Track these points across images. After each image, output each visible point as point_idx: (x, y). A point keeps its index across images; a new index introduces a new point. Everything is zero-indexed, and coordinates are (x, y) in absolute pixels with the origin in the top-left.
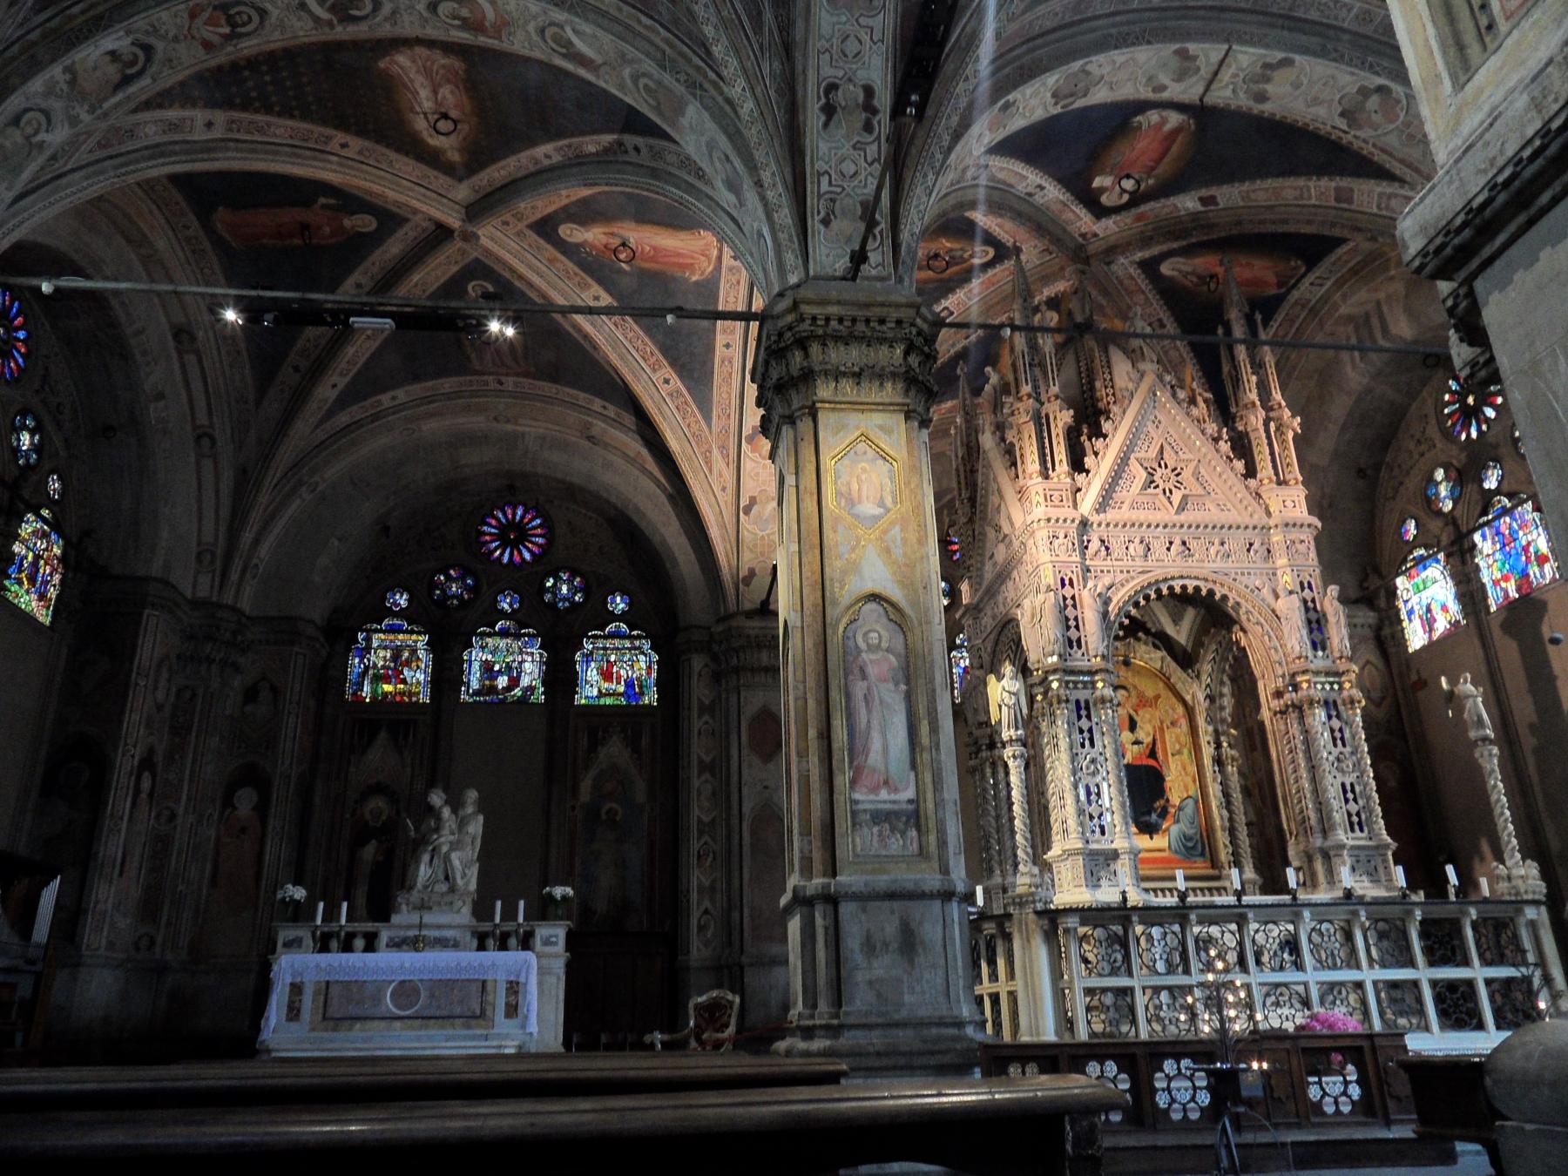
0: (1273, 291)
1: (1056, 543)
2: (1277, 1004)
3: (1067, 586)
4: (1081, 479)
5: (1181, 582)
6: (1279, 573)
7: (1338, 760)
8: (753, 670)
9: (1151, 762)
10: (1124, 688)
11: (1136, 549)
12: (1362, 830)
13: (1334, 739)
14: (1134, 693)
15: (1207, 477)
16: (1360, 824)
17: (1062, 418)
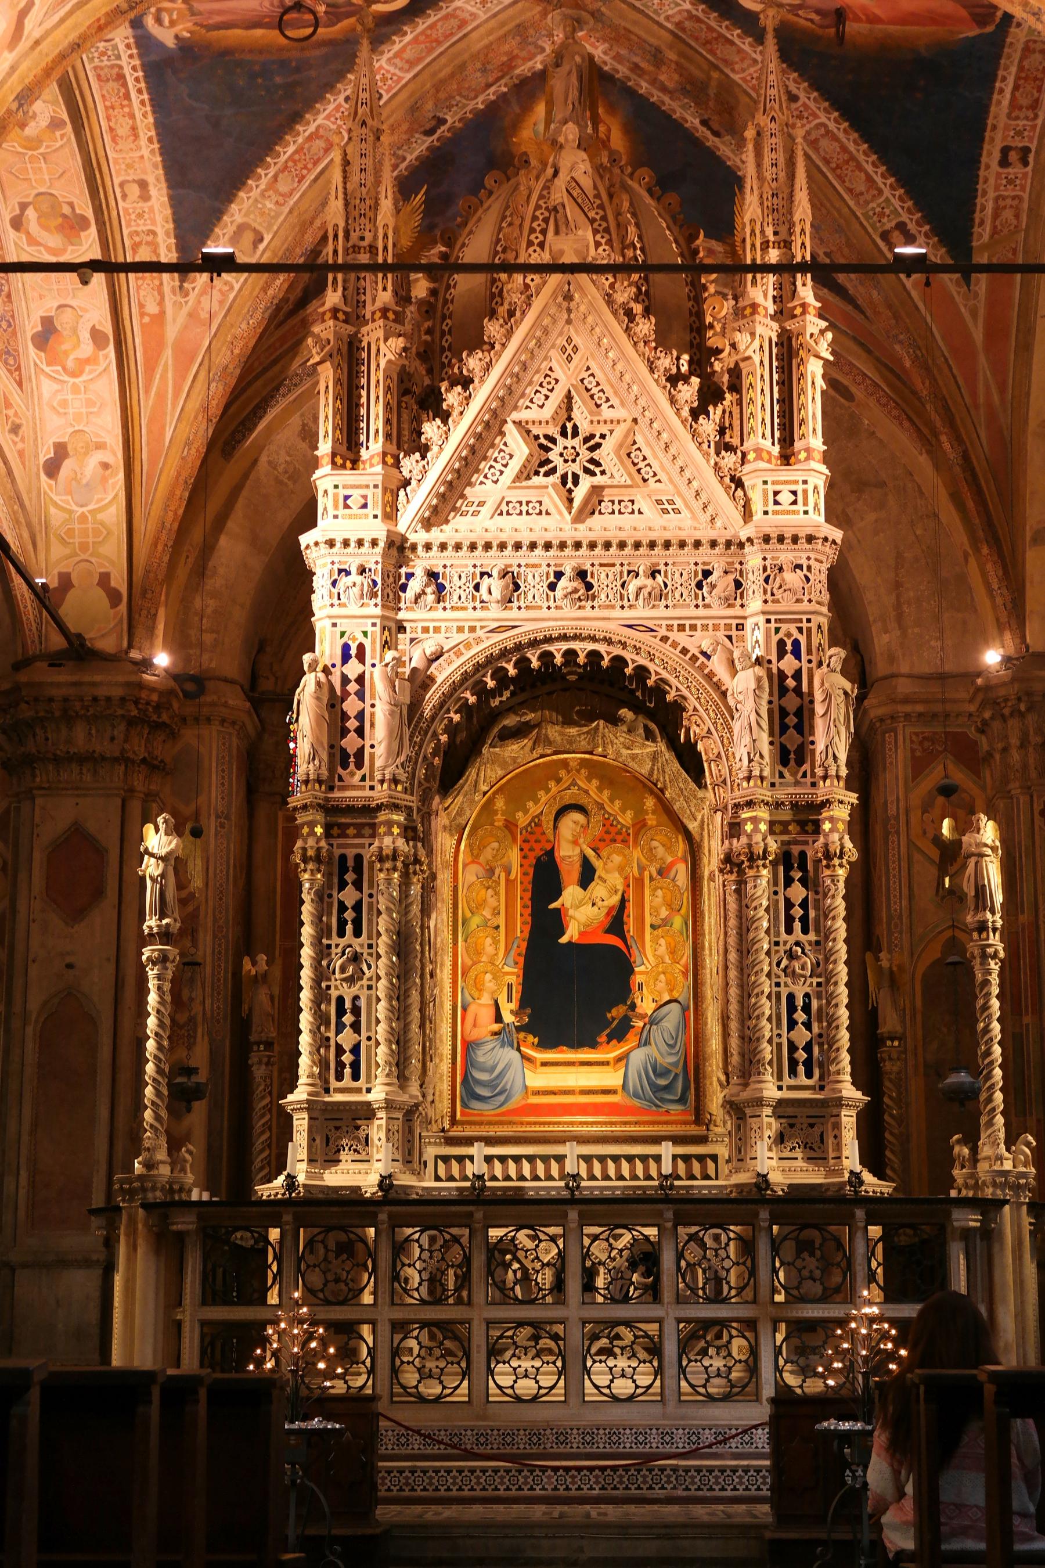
0: (974, 32)
1: (344, 581)
2: (608, 1352)
3: (353, 662)
4: (410, 464)
5: (564, 646)
6: (749, 624)
7: (791, 956)
8: (57, 760)
9: (613, 940)
10: (581, 809)
11: (496, 586)
12: (809, 1075)
13: (789, 920)
14: (597, 818)
15: (647, 451)
16: (808, 1064)
17: (385, 350)
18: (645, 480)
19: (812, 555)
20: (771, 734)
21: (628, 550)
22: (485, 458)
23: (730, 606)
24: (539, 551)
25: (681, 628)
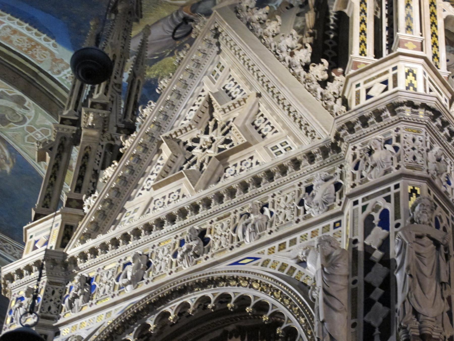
18: (264, 136)
19: (401, 126)
20: (354, 315)
21: (239, 196)
22: (144, 175)
23: (329, 209)
24: (167, 227)
25: (282, 247)
